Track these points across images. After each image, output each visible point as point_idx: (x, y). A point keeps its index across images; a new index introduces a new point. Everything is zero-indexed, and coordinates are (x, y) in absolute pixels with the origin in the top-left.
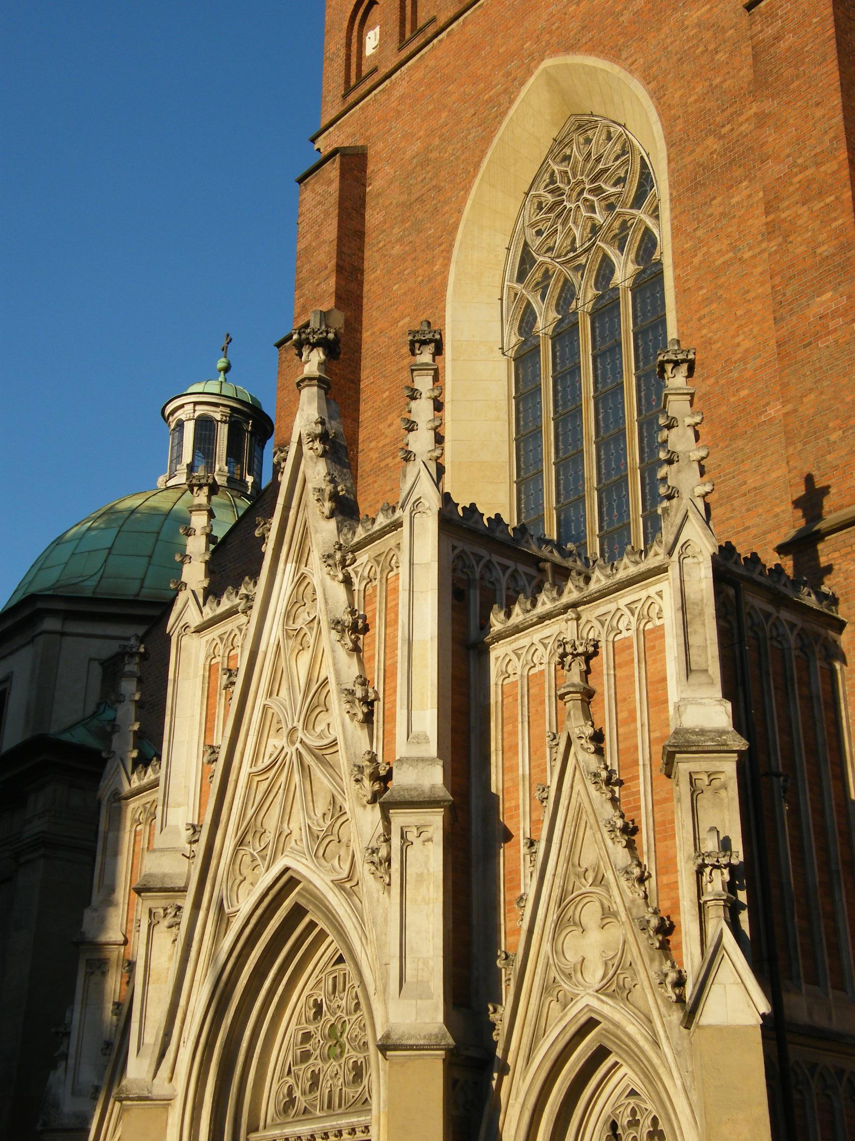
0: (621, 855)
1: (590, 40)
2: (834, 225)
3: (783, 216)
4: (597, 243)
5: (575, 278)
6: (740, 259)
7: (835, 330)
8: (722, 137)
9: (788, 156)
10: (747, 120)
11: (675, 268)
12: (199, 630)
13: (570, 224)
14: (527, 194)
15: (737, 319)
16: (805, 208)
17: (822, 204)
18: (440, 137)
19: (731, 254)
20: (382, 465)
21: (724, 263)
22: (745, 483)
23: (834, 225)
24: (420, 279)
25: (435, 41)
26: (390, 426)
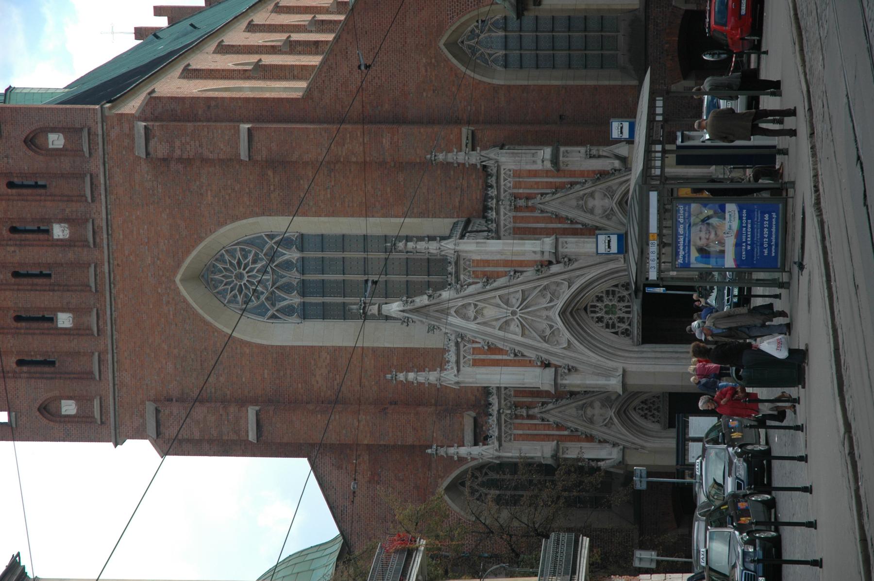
0: (578, 187)
1: (182, 253)
2: (359, 135)
3: (344, 154)
4: (273, 266)
5: (282, 281)
6: (333, 186)
7: (398, 139)
8: (274, 191)
9: (321, 150)
10: (274, 178)
11: (320, 216)
12: (458, 371)
13: (255, 281)
14: (225, 306)
15: (357, 190)
16: (346, 146)
17: (348, 139)
18: (175, 349)
19: (329, 190)
20: (336, 387)
21: (330, 194)
22: (424, 193)
23: (359, 135)
24: (248, 362)
25: (115, 351)
26: (318, 383)
